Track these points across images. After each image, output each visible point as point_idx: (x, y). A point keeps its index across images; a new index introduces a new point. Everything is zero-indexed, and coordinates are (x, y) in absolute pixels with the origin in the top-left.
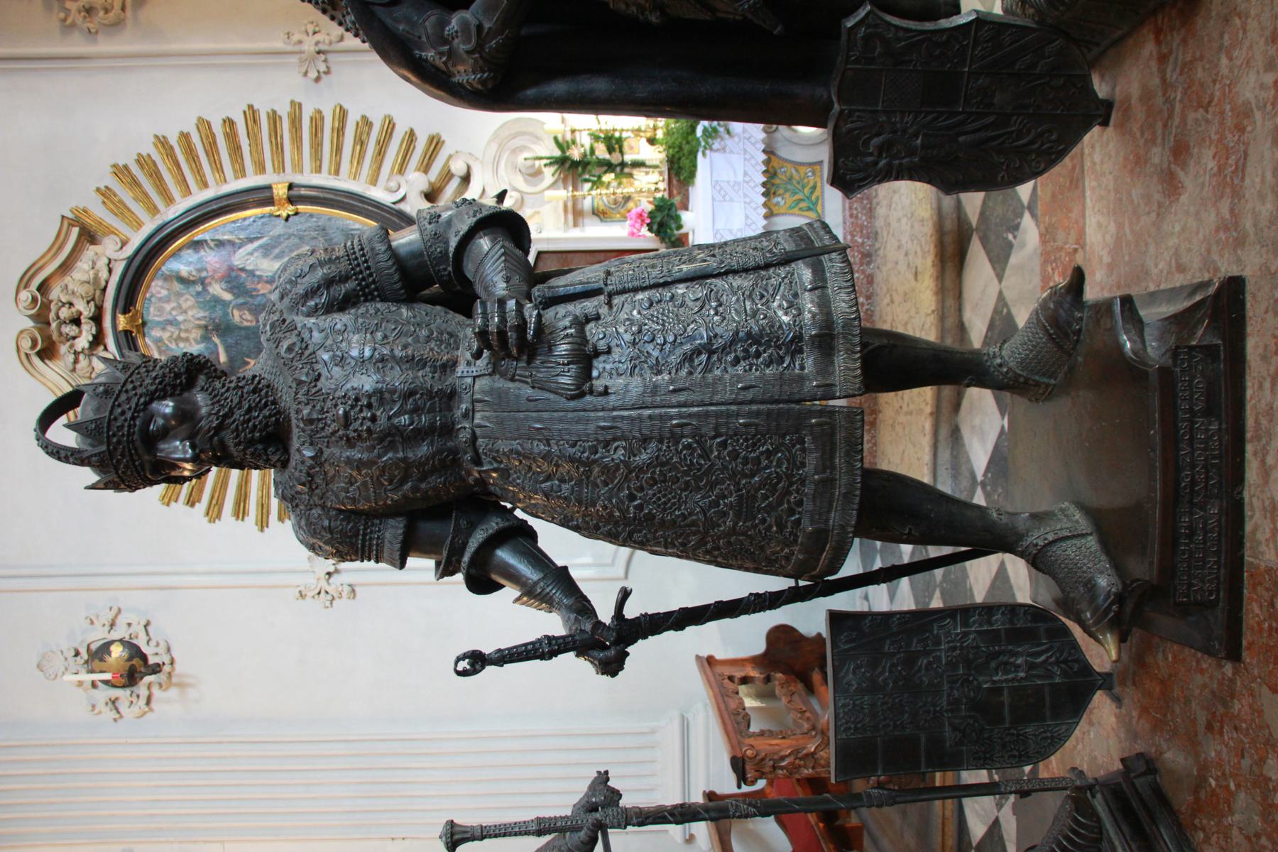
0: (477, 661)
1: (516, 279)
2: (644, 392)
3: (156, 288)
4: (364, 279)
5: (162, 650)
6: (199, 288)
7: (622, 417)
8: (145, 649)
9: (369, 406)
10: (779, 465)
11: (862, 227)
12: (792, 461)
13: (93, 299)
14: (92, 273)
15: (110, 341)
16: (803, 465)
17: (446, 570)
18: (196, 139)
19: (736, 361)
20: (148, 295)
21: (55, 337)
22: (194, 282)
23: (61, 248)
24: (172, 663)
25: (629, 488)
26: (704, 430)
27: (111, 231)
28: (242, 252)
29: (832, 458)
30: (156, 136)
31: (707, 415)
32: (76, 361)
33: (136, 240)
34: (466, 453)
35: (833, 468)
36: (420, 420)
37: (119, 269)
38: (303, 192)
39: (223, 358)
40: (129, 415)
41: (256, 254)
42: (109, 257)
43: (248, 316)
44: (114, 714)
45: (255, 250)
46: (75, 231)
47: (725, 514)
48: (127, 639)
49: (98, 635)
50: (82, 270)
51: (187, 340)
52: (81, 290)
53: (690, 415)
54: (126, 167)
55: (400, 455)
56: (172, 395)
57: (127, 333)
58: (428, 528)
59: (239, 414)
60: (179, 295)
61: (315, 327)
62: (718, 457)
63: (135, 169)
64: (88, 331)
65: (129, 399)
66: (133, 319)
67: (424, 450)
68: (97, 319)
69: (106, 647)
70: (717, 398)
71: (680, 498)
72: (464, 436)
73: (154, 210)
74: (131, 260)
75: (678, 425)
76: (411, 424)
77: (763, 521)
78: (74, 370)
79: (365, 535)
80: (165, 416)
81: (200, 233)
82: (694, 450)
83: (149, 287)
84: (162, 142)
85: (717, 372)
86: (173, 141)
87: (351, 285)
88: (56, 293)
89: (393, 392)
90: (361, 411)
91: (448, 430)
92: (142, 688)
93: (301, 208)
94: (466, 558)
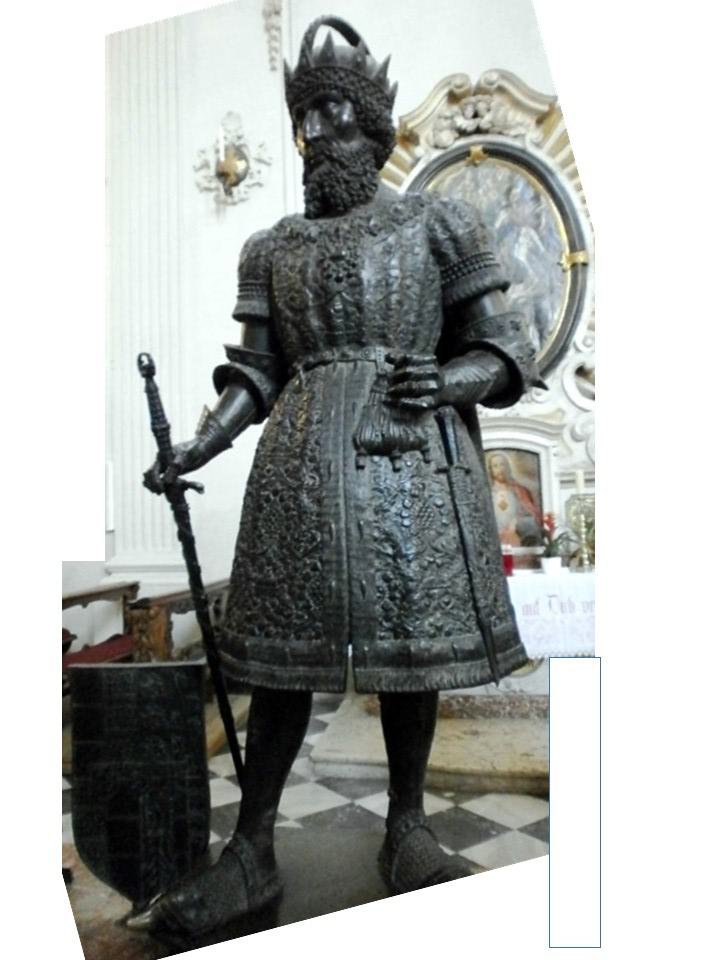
0: (148, 371)
1: (459, 392)
2: (358, 499)
3: (502, 171)
4: (460, 269)
5: (243, 196)
6: (504, 203)
7: (337, 481)
8: (242, 185)
9: (349, 276)
10: (299, 617)
12: (303, 628)
13: (493, 126)
14: (513, 123)
15: (463, 142)
16: (298, 638)
17: (231, 352)
19: (387, 579)
21: (464, 101)
24: (234, 204)
25: (283, 490)
26: (327, 551)
28: (533, 232)
29: (303, 664)
31: (339, 553)
32: (446, 118)
33: (541, 155)
34: (314, 357)
35: (296, 664)
36: (339, 318)
37: (517, 143)
38: (580, 277)
40: (340, 84)
41: (531, 243)
42: (525, 136)
44: (198, 165)
45: (535, 243)
46: (545, 108)
47: (261, 569)
48: (250, 171)
49: (252, 152)
50: (515, 116)
53: (338, 539)
55: (311, 303)
56: (358, 119)
57: (468, 153)
58: (262, 334)
59: (344, 174)
60: (498, 189)
61: (414, 233)
62: (305, 565)
64: (468, 124)
65: (352, 83)
66: (478, 157)
67: (315, 323)
69: (242, 156)
70: (354, 562)
71: (275, 533)
72: (327, 355)
74: (524, 151)
75: (330, 528)
76: (335, 310)
77: (255, 604)
78: (440, 117)
79: (255, 285)
80: (340, 114)
81: (547, 201)
82: (311, 543)
83: (505, 166)
85: (377, 563)
87: (453, 257)
88: (497, 99)
89: (361, 294)
90: (345, 269)
91: (332, 342)
92: (216, 184)
93: (569, 273)
94: (238, 365)
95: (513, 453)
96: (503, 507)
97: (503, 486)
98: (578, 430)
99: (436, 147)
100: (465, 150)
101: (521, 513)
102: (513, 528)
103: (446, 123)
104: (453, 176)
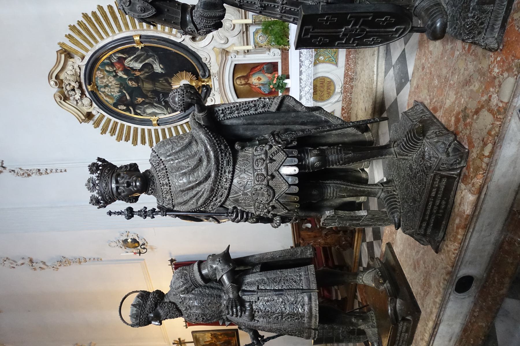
11: (351, 69)
13: (77, 81)
14: (73, 70)
18: (98, 14)
20: (96, 77)
21: (67, 96)
22: (112, 72)
23: (60, 62)
27: (77, 52)
30: (83, 13)
32: (77, 103)
37: (83, 69)
39: (128, 98)
42: (78, 65)
43: (134, 83)
46: (63, 56)
51: (114, 92)
52: (72, 78)
54: (74, 26)
57: (92, 92)
63: (78, 27)
64: (78, 92)
68: (80, 87)
73: (91, 45)
74: (87, 65)
83: (96, 74)
84: (85, 16)
86: (90, 15)
95: (235, 75)
96: (259, 79)
97: (250, 79)
98: (223, 42)
99: (91, 105)
100: (91, 93)
101: (261, 71)
102: (269, 75)
103: (80, 103)
104: (105, 98)
